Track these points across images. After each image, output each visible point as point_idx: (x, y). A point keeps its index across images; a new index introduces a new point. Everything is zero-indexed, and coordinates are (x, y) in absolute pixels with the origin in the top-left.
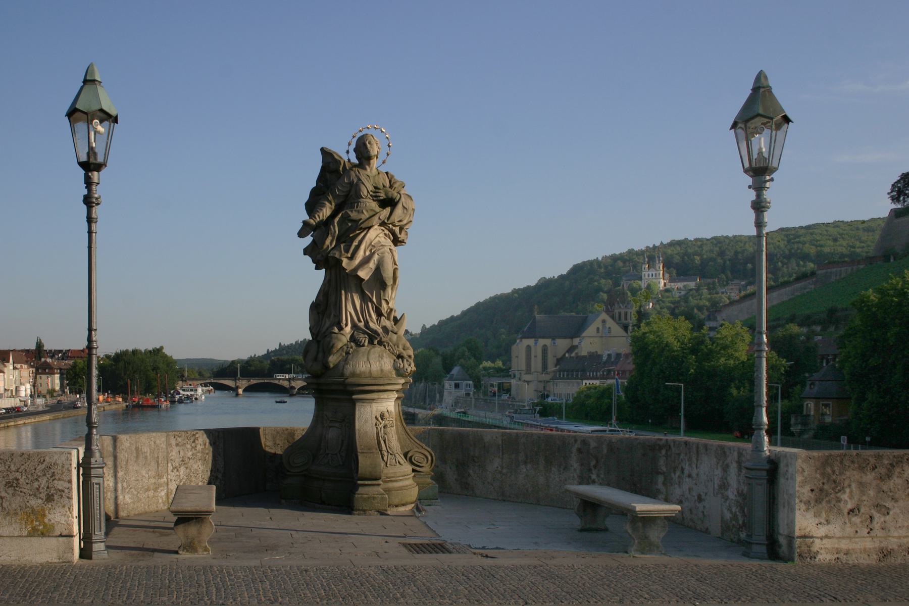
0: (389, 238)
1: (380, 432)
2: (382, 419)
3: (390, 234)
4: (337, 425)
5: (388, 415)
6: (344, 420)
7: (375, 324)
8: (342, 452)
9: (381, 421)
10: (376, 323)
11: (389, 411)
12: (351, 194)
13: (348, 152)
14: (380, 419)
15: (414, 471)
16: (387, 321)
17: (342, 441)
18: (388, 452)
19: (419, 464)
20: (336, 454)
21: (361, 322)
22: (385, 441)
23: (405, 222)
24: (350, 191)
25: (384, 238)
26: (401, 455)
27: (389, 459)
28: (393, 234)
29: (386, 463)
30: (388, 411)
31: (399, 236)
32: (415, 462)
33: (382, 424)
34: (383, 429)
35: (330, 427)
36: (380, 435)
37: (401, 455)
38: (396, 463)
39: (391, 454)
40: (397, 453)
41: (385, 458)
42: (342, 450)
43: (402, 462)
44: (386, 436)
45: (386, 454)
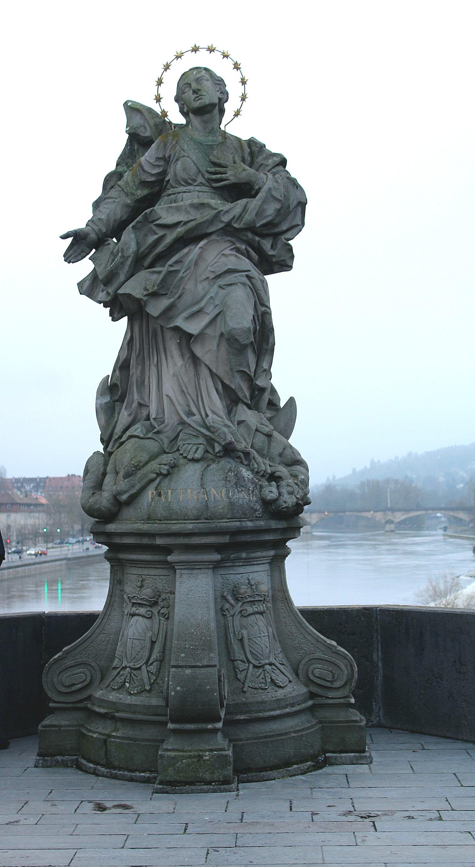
0: (249, 258)
1: (230, 625)
2: (237, 600)
3: (250, 249)
4: (142, 611)
5: (249, 590)
6: (156, 603)
7: (222, 418)
8: (151, 664)
9: (232, 602)
10: (224, 417)
11: (252, 582)
12: (167, 179)
13: (158, 99)
14: (229, 598)
15: (312, 695)
16: (249, 412)
17: (153, 643)
18: (249, 662)
19: (329, 684)
20: (139, 668)
21: (194, 415)
22: (241, 640)
23: (284, 228)
24: (164, 173)
25: (236, 256)
26: (281, 667)
27: (249, 675)
28: (259, 250)
29: (243, 684)
30: (249, 583)
31: (271, 253)
32: (315, 680)
33: (235, 609)
34: (237, 618)
35: (133, 615)
36: (231, 630)
37: (281, 667)
38: (266, 683)
39: (255, 666)
40: (270, 664)
41: (241, 676)
42: (149, 663)
43: (281, 679)
44: (245, 632)
45: (242, 666)
